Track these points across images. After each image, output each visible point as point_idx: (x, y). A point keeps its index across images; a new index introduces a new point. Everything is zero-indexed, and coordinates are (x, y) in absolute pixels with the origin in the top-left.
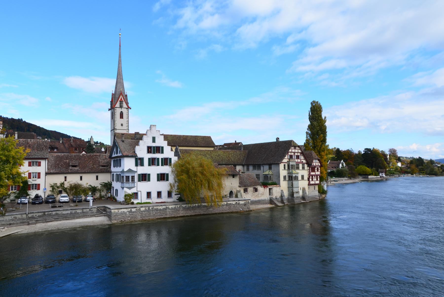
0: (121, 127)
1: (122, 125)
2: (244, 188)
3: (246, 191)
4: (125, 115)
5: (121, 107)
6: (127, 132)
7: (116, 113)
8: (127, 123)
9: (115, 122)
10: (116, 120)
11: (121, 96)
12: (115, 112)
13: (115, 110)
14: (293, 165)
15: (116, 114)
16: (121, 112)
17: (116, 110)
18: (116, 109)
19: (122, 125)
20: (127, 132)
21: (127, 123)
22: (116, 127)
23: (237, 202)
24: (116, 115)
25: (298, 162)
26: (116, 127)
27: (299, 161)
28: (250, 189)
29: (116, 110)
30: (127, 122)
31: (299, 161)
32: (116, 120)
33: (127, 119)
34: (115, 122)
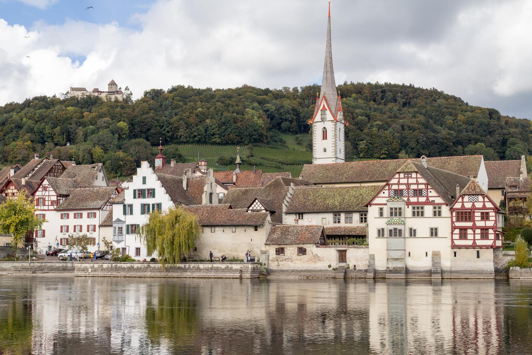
0: (323, 155)
1: (325, 150)
2: (277, 247)
3: (280, 251)
4: (330, 134)
5: (323, 120)
6: (333, 161)
7: (316, 131)
8: (332, 147)
9: (315, 146)
10: (316, 144)
11: (323, 102)
12: (315, 129)
13: (315, 127)
14: (396, 209)
15: (316, 134)
16: (325, 128)
17: (316, 126)
18: (315, 124)
19: (325, 150)
20: (333, 161)
21: (332, 147)
22: (316, 154)
23: (229, 265)
24: (315, 135)
25: (418, 203)
26: (316, 154)
27: (422, 199)
28: (291, 251)
29: (316, 126)
30: (333, 144)
31: (422, 199)
32: (316, 144)
33: (333, 139)
34: (315, 146)
